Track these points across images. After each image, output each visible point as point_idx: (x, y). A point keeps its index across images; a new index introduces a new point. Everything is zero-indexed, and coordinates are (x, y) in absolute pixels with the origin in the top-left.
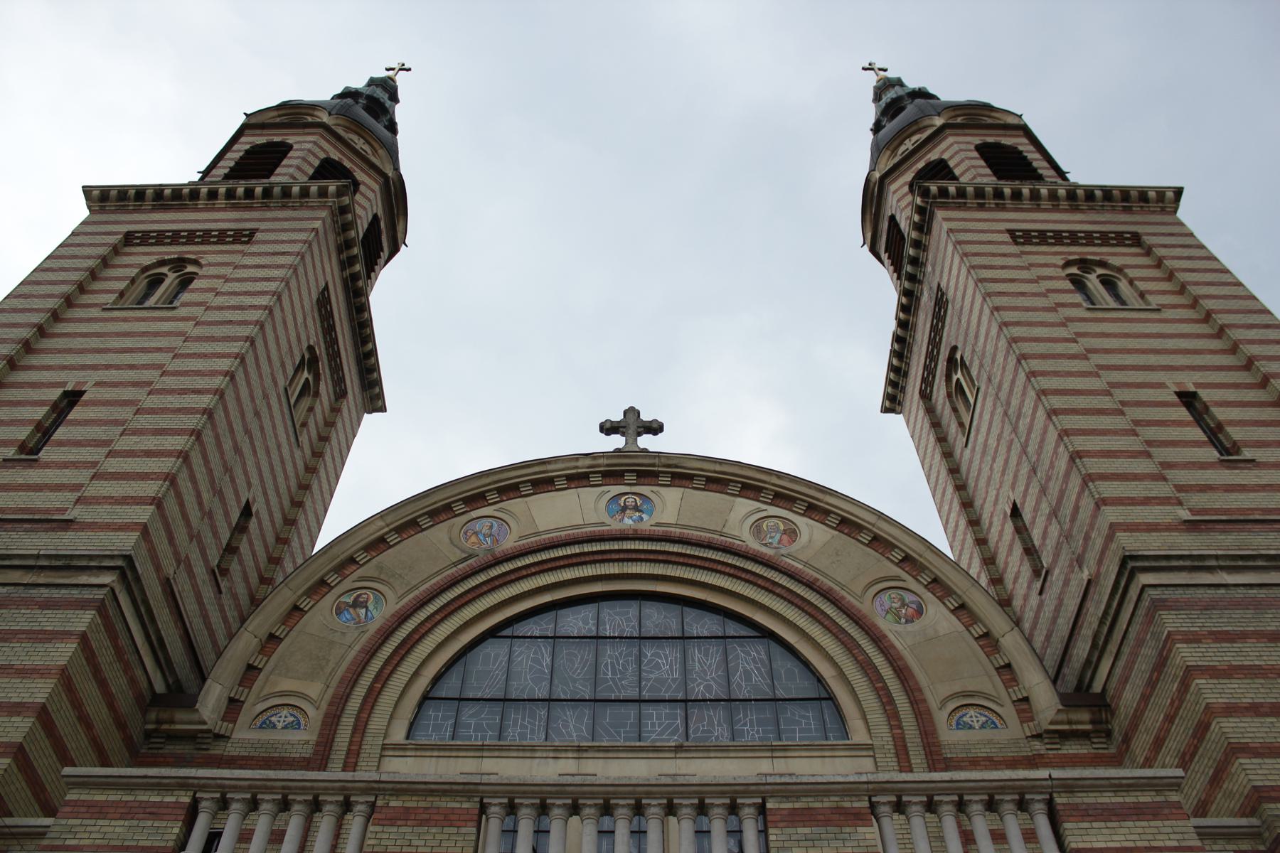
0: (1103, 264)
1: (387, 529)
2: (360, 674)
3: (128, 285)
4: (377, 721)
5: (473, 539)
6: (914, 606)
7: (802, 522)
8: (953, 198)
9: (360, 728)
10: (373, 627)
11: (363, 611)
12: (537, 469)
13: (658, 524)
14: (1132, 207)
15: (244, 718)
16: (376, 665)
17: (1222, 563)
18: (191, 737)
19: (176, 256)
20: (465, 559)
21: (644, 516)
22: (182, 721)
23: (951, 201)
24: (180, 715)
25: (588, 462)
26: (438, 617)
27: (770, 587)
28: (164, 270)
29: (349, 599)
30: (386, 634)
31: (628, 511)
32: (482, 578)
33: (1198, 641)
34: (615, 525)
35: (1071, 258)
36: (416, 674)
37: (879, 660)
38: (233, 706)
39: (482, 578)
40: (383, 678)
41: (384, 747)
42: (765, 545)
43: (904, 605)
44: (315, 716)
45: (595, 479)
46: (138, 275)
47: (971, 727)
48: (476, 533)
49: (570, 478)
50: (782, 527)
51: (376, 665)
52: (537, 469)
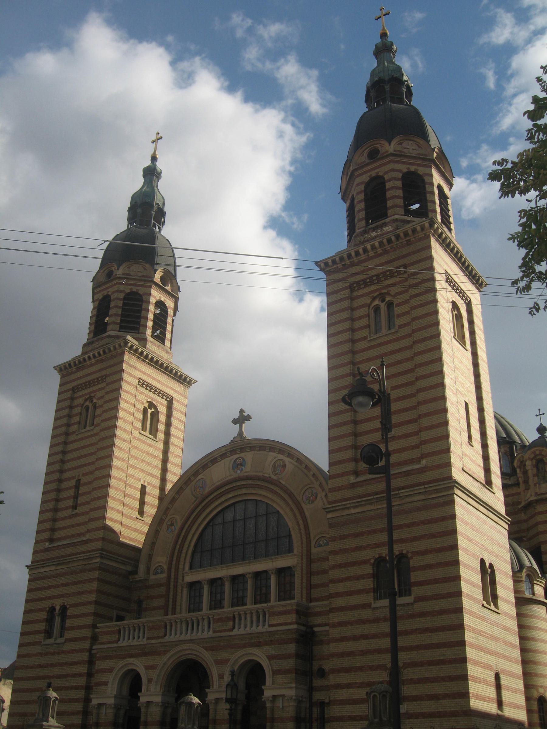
0: (388, 294)
1: (174, 494)
2: (174, 551)
3: (80, 417)
4: (181, 566)
5: (198, 490)
6: (315, 495)
7: (287, 460)
8: (332, 266)
9: (177, 569)
10: (176, 532)
11: (173, 527)
12: (210, 456)
13: (246, 472)
14: (410, 239)
15: (151, 572)
16: (178, 546)
17: (352, 505)
18: (140, 581)
19: (88, 396)
20: (196, 500)
21: (243, 468)
22: (137, 578)
23: (331, 268)
24: (136, 576)
25: (224, 449)
26: (191, 525)
27: (276, 493)
28: (87, 403)
29: (169, 523)
30: (178, 536)
31: (239, 467)
32: (200, 507)
33: (335, 540)
34: (235, 475)
35: (375, 295)
36: (189, 546)
37: (301, 522)
38: (148, 569)
39: (200, 507)
40: (180, 552)
41: (183, 574)
42: (276, 474)
43: (312, 495)
44: (165, 567)
45: (229, 454)
46: (81, 410)
47: (321, 546)
48: (199, 487)
49: (221, 456)
50: (282, 464)
51: (178, 546)
52: (210, 456)
